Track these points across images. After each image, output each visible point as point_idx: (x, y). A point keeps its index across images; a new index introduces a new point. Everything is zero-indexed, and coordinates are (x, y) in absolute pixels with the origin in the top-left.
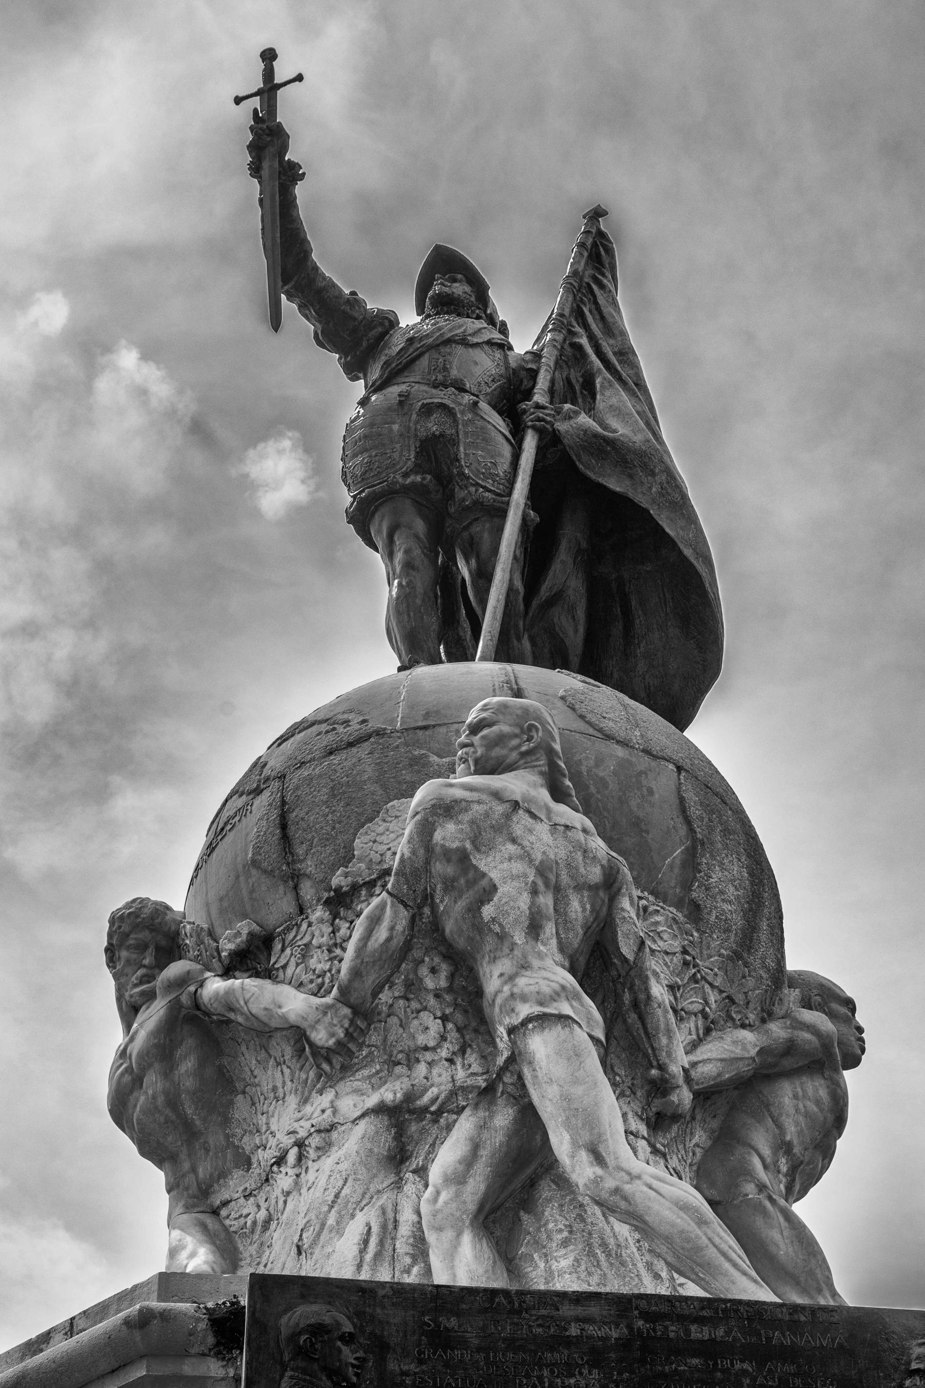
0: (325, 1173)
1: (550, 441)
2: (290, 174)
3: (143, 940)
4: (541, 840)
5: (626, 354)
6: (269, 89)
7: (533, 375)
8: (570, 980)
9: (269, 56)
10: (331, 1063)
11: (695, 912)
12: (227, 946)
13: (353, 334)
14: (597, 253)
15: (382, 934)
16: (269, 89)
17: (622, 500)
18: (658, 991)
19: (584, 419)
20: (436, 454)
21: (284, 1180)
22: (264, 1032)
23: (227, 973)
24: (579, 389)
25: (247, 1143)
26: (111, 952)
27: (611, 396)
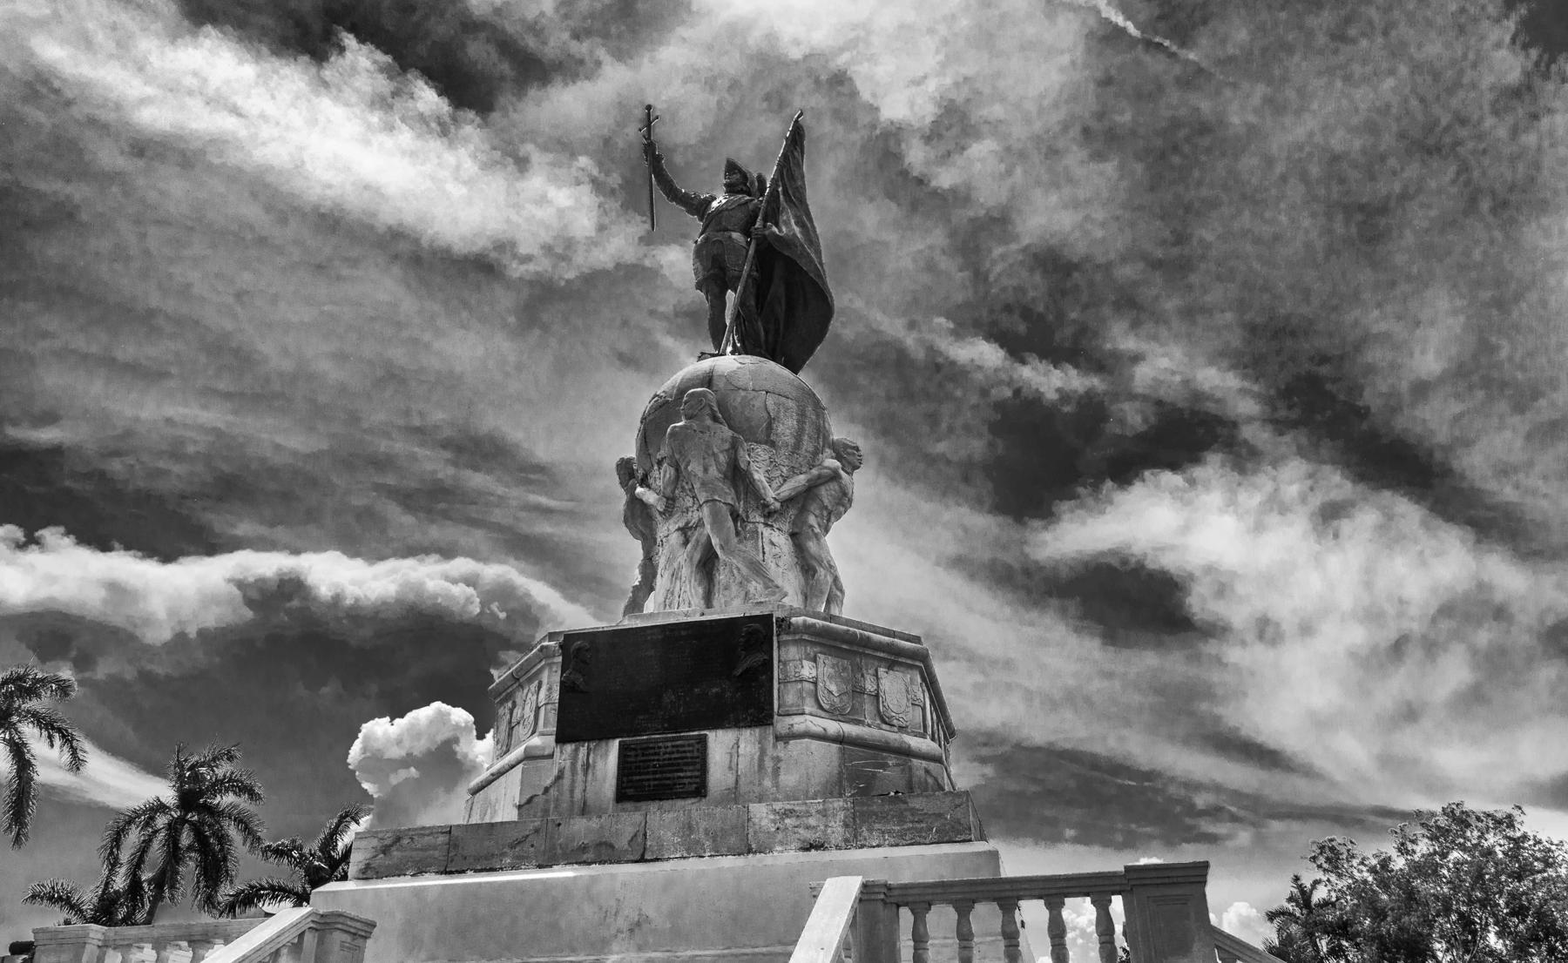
11: (773, 444)
14: (797, 138)
18: (759, 476)
19: (775, 229)
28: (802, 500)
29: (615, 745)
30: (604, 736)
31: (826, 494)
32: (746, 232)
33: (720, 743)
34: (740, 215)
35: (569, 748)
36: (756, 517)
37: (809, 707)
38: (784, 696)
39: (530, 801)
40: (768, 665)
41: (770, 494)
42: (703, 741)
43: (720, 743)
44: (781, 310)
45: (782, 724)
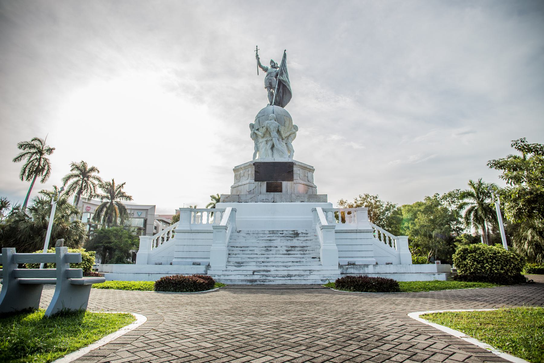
0: (263, 144)
3: (252, 126)
4: (274, 125)
5: (286, 69)
8: (276, 134)
10: (263, 137)
13: (265, 70)
18: (282, 132)
20: (270, 84)
24: (282, 74)
27: (285, 75)
28: (288, 137)
29: (266, 182)
30: (263, 181)
31: (292, 136)
32: (276, 78)
33: (284, 184)
34: (275, 74)
35: (257, 182)
36: (280, 140)
37: (299, 178)
38: (295, 177)
40: (292, 171)
41: (284, 136)
42: (281, 183)
43: (284, 184)
44: (281, 95)
45: (295, 181)
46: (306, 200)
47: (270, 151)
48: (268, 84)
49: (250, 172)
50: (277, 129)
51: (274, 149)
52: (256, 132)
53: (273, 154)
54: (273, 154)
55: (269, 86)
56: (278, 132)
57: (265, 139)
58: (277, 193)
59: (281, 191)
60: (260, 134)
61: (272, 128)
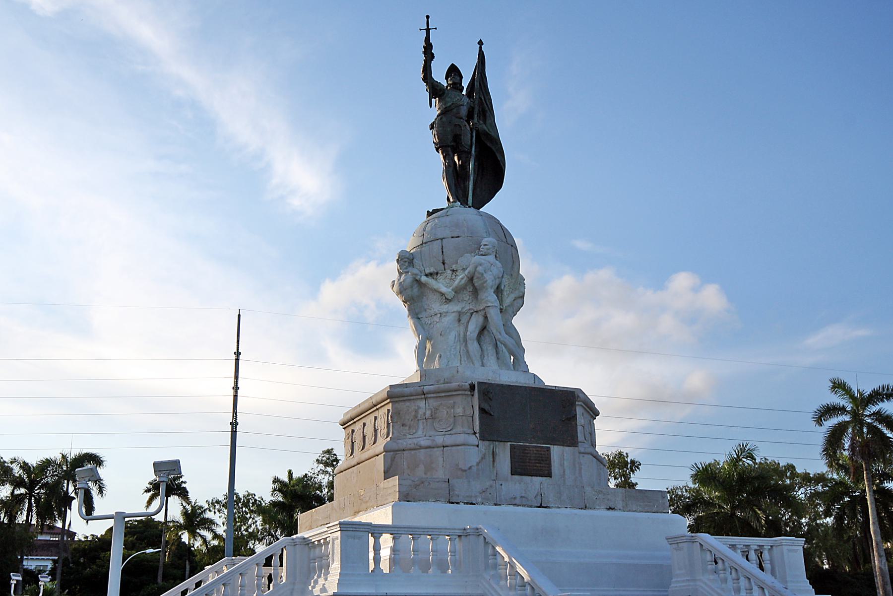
1: (477, 132)
2: (433, 56)
3: (406, 261)
6: (428, 30)
7: (473, 108)
9: (428, 17)
10: (448, 301)
12: (427, 271)
13: (435, 91)
15: (463, 282)
16: (428, 30)
17: (489, 148)
20: (457, 138)
21: (436, 319)
22: (436, 291)
23: (426, 275)
25: (426, 307)
26: (398, 260)
33: (556, 451)
39: (470, 468)
42: (548, 449)
43: (556, 451)
46: (620, 505)
47: (474, 346)
48: (450, 137)
49: (459, 411)
50: (497, 282)
51: (486, 339)
52: (424, 279)
53: (482, 356)
54: (482, 356)
55: (448, 142)
56: (498, 291)
57: (455, 307)
58: (539, 479)
59: (549, 475)
60: (443, 289)
61: (490, 279)
